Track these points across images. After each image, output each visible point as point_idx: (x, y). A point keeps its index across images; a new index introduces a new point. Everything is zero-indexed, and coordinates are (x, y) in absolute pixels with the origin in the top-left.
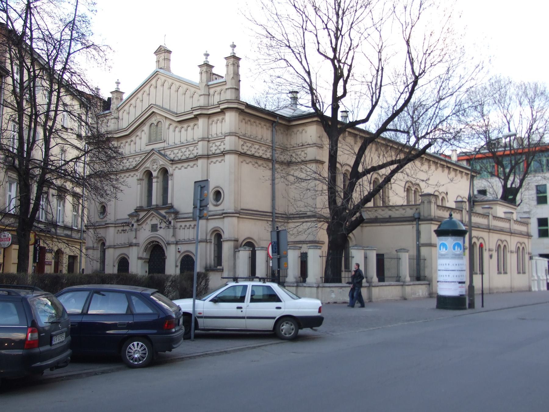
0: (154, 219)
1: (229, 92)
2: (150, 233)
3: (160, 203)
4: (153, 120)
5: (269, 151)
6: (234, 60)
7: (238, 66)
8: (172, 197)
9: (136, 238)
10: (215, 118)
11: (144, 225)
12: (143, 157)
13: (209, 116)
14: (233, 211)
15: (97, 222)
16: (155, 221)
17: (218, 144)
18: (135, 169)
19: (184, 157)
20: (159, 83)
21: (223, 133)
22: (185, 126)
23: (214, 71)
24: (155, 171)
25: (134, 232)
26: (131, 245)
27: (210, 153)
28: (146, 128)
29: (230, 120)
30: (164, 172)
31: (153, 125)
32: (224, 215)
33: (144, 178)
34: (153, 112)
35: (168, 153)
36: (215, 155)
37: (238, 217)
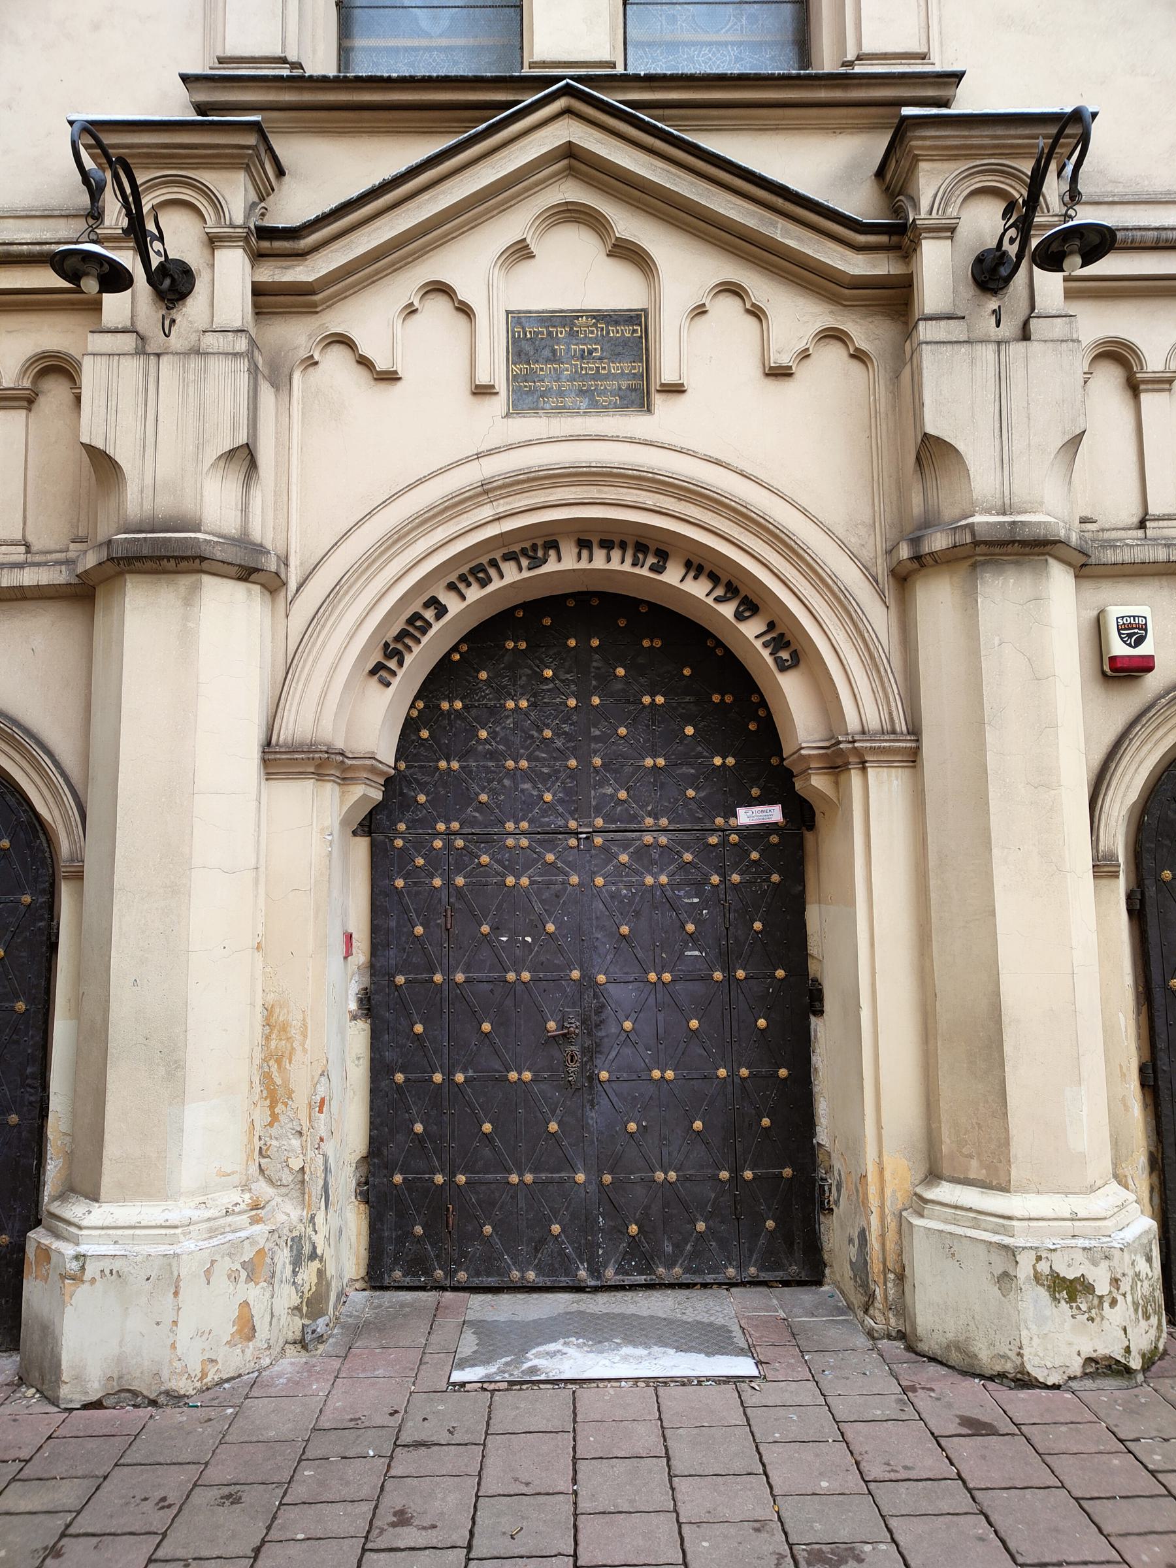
2: (492, 422)
9: (244, 458)
11: (371, 319)
16: (574, 276)
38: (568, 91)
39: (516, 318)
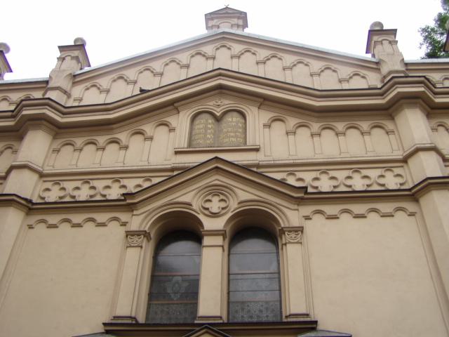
8: (309, 294)
24: (215, 215)
38: (206, 327)
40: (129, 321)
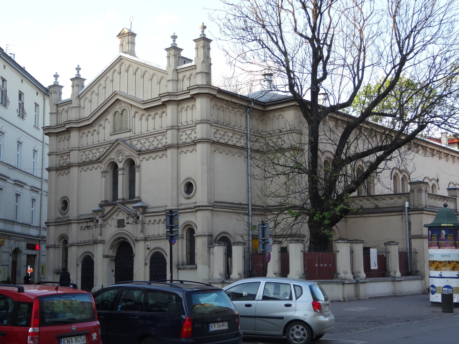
0: (121, 214)
1: (199, 76)
2: (116, 229)
3: (126, 196)
4: (118, 108)
5: (242, 139)
6: (204, 42)
7: (209, 49)
9: (101, 234)
10: (185, 105)
11: (109, 221)
12: (107, 148)
13: (179, 102)
14: (207, 204)
15: (58, 218)
16: (121, 216)
17: (188, 132)
18: (98, 161)
19: (151, 147)
20: (124, 68)
21: (194, 120)
22: (153, 113)
23: (183, 54)
24: (121, 162)
25: (99, 229)
26: (96, 242)
27: (181, 142)
28: (110, 117)
29: (201, 107)
30: (131, 163)
31: (117, 113)
32: (197, 209)
33: (109, 169)
34: (118, 99)
35: (134, 143)
36: (186, 145)
37: (212, 210)
39: (118, 220)
40: (103, 203)
